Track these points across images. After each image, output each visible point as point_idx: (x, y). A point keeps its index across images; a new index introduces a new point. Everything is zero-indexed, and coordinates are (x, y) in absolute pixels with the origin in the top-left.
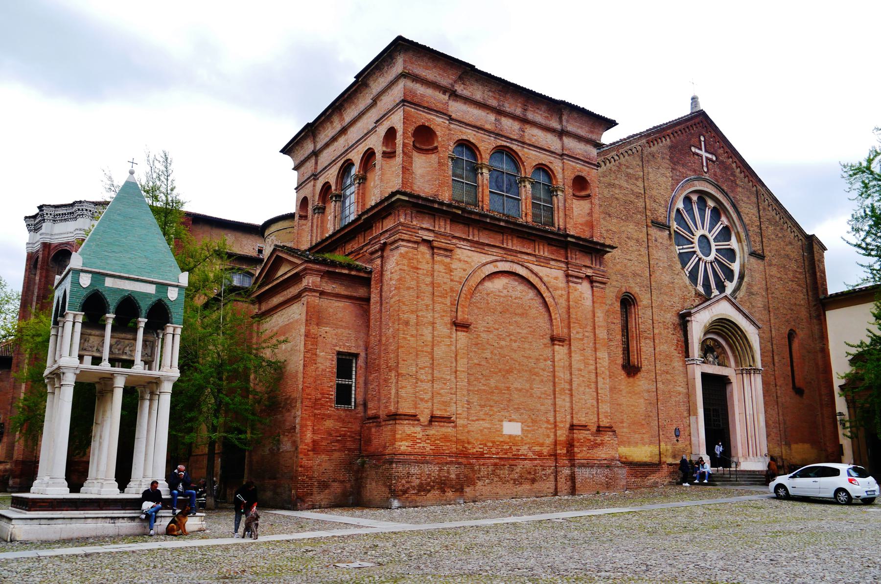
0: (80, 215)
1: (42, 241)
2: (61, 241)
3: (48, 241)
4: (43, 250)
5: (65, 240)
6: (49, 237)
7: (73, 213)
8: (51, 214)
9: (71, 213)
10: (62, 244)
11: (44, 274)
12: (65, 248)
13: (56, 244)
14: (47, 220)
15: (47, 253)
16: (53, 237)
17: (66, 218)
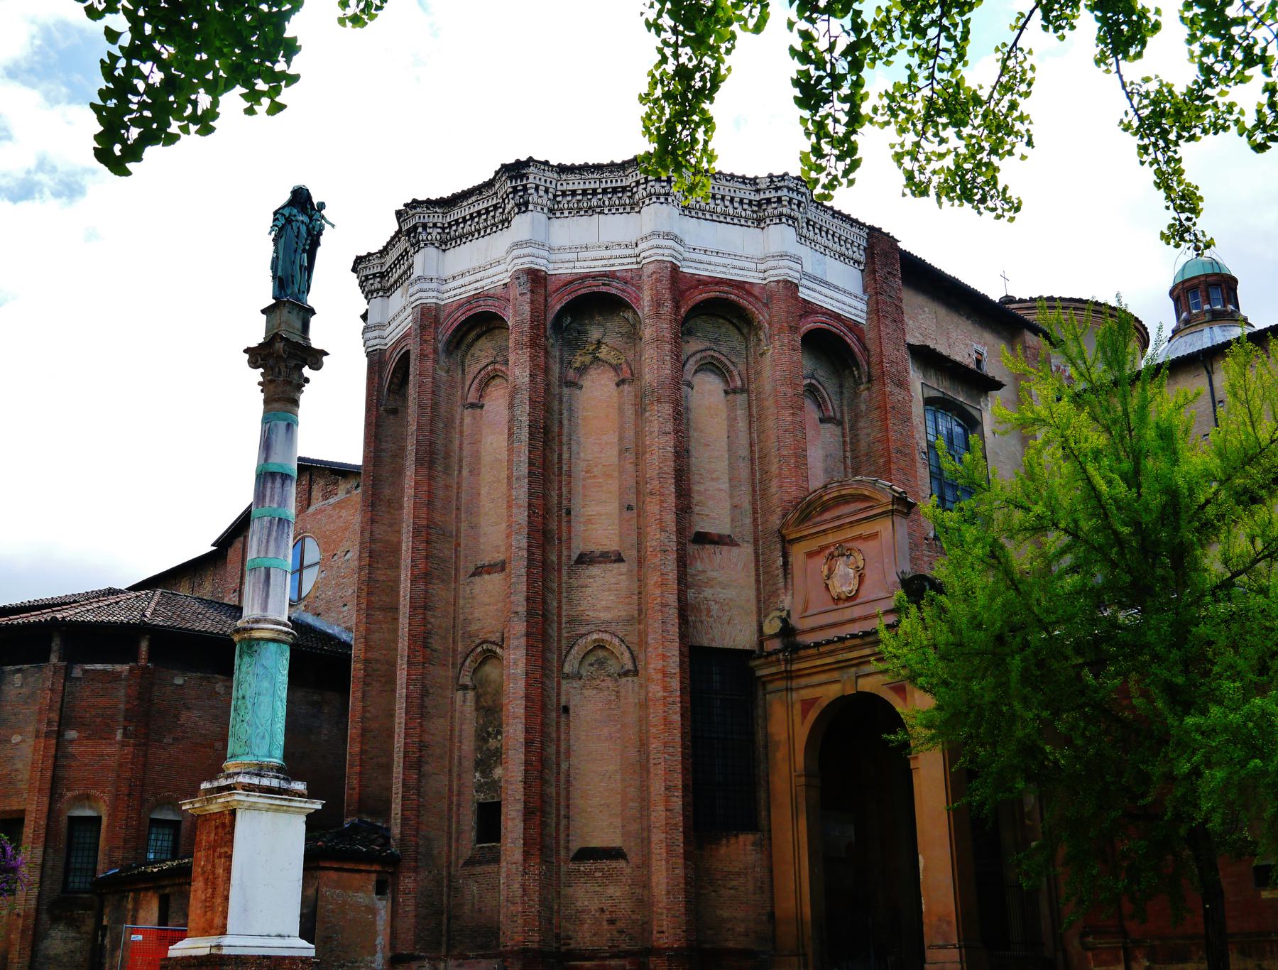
0: (658, 196)
1: (525, 263)
2: (582, 268)
3: (541, 265)
4: (532, 291)
5: (599, 267)
6: (545, 254)
7: (624, 189)
8: (546, 191)
9: (615, 190)
10: (594, 277)
11: (541, 361)
12: (603, 289)
13: (569, 278)
14: (536, 204)
15: (541, 300)
16: (553, 258)
17: (595, 202)
